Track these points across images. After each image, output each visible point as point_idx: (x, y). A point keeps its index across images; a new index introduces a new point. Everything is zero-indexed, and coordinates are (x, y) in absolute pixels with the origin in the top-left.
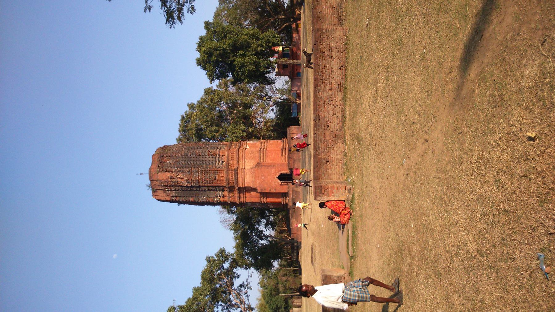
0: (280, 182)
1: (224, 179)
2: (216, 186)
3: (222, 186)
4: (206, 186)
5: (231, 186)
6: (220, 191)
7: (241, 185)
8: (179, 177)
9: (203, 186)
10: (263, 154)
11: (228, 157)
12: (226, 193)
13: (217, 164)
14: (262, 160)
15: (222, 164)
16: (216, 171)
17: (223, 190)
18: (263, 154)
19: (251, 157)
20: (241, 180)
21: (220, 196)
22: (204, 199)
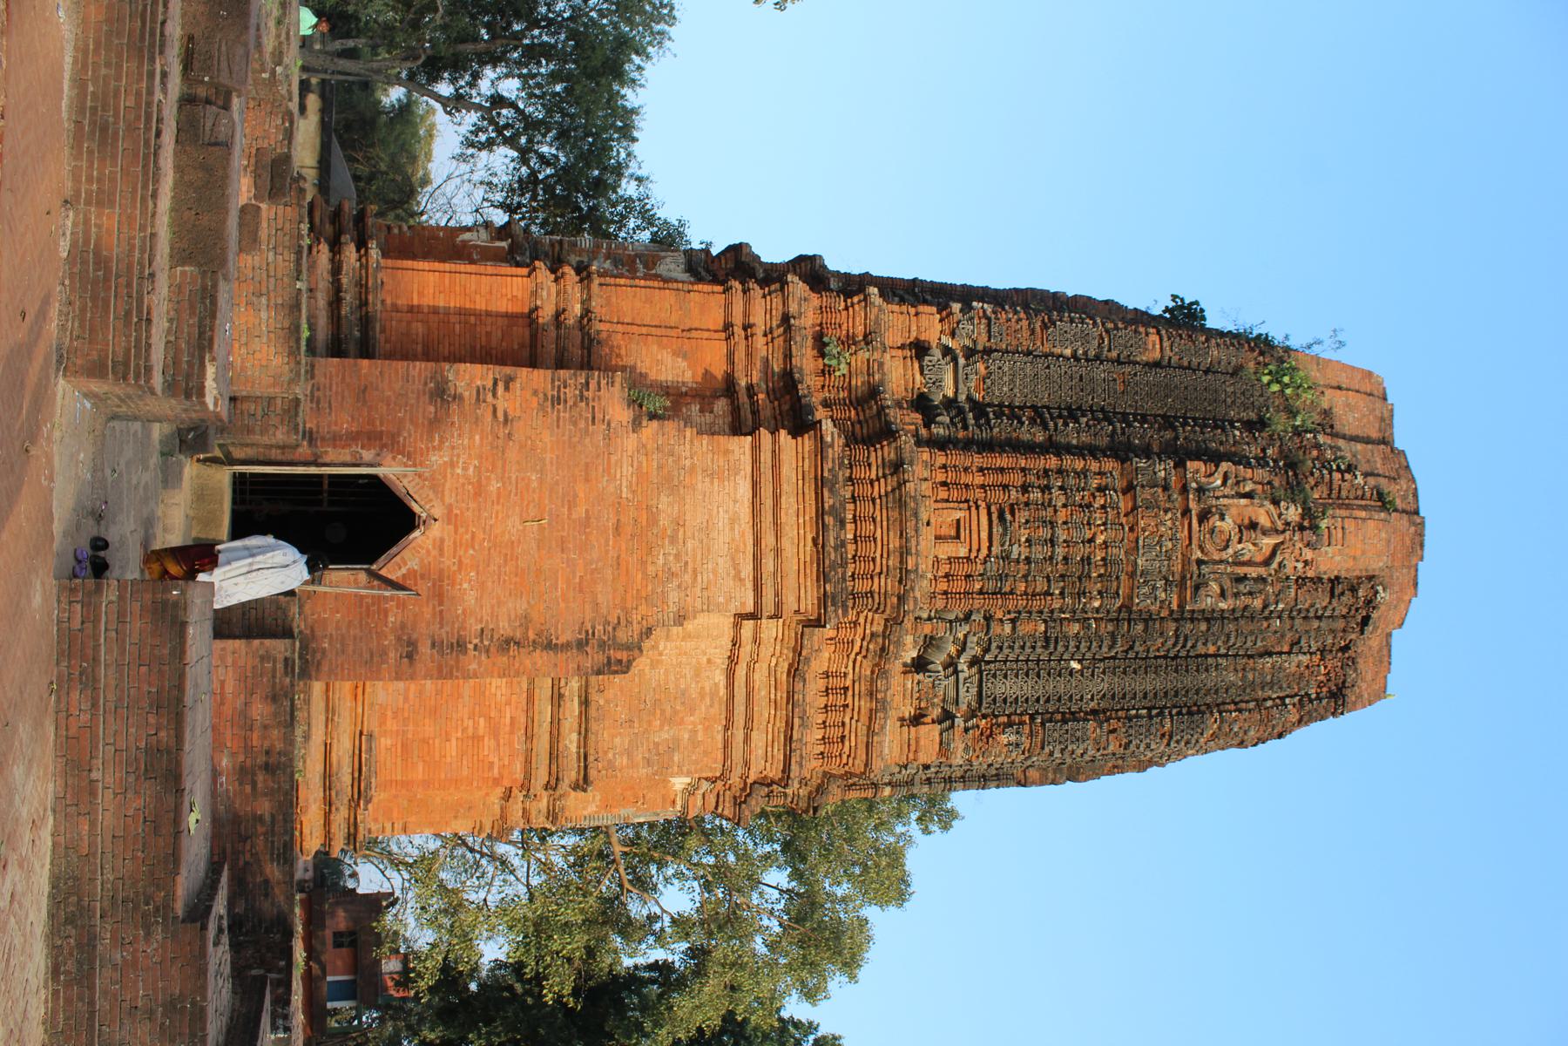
0: (390, 470)
1: (936, 516)
2: (987, 446)
3: (941, 444)
5: (870, 441)
6: (950, 403)
7: (791, 450)
8: (1268, 542)
9: (1092, 451)
10: (554, 755)
11: (880, 706)
12: (899, 377)
13: (974, 649)
14: (573, 686)
15: (930, 642)
17: (921, 403)
18: (554, 755)
19: (669, 721)
20: (789, 502)
21: (947, 351)
22: (1065, 341)
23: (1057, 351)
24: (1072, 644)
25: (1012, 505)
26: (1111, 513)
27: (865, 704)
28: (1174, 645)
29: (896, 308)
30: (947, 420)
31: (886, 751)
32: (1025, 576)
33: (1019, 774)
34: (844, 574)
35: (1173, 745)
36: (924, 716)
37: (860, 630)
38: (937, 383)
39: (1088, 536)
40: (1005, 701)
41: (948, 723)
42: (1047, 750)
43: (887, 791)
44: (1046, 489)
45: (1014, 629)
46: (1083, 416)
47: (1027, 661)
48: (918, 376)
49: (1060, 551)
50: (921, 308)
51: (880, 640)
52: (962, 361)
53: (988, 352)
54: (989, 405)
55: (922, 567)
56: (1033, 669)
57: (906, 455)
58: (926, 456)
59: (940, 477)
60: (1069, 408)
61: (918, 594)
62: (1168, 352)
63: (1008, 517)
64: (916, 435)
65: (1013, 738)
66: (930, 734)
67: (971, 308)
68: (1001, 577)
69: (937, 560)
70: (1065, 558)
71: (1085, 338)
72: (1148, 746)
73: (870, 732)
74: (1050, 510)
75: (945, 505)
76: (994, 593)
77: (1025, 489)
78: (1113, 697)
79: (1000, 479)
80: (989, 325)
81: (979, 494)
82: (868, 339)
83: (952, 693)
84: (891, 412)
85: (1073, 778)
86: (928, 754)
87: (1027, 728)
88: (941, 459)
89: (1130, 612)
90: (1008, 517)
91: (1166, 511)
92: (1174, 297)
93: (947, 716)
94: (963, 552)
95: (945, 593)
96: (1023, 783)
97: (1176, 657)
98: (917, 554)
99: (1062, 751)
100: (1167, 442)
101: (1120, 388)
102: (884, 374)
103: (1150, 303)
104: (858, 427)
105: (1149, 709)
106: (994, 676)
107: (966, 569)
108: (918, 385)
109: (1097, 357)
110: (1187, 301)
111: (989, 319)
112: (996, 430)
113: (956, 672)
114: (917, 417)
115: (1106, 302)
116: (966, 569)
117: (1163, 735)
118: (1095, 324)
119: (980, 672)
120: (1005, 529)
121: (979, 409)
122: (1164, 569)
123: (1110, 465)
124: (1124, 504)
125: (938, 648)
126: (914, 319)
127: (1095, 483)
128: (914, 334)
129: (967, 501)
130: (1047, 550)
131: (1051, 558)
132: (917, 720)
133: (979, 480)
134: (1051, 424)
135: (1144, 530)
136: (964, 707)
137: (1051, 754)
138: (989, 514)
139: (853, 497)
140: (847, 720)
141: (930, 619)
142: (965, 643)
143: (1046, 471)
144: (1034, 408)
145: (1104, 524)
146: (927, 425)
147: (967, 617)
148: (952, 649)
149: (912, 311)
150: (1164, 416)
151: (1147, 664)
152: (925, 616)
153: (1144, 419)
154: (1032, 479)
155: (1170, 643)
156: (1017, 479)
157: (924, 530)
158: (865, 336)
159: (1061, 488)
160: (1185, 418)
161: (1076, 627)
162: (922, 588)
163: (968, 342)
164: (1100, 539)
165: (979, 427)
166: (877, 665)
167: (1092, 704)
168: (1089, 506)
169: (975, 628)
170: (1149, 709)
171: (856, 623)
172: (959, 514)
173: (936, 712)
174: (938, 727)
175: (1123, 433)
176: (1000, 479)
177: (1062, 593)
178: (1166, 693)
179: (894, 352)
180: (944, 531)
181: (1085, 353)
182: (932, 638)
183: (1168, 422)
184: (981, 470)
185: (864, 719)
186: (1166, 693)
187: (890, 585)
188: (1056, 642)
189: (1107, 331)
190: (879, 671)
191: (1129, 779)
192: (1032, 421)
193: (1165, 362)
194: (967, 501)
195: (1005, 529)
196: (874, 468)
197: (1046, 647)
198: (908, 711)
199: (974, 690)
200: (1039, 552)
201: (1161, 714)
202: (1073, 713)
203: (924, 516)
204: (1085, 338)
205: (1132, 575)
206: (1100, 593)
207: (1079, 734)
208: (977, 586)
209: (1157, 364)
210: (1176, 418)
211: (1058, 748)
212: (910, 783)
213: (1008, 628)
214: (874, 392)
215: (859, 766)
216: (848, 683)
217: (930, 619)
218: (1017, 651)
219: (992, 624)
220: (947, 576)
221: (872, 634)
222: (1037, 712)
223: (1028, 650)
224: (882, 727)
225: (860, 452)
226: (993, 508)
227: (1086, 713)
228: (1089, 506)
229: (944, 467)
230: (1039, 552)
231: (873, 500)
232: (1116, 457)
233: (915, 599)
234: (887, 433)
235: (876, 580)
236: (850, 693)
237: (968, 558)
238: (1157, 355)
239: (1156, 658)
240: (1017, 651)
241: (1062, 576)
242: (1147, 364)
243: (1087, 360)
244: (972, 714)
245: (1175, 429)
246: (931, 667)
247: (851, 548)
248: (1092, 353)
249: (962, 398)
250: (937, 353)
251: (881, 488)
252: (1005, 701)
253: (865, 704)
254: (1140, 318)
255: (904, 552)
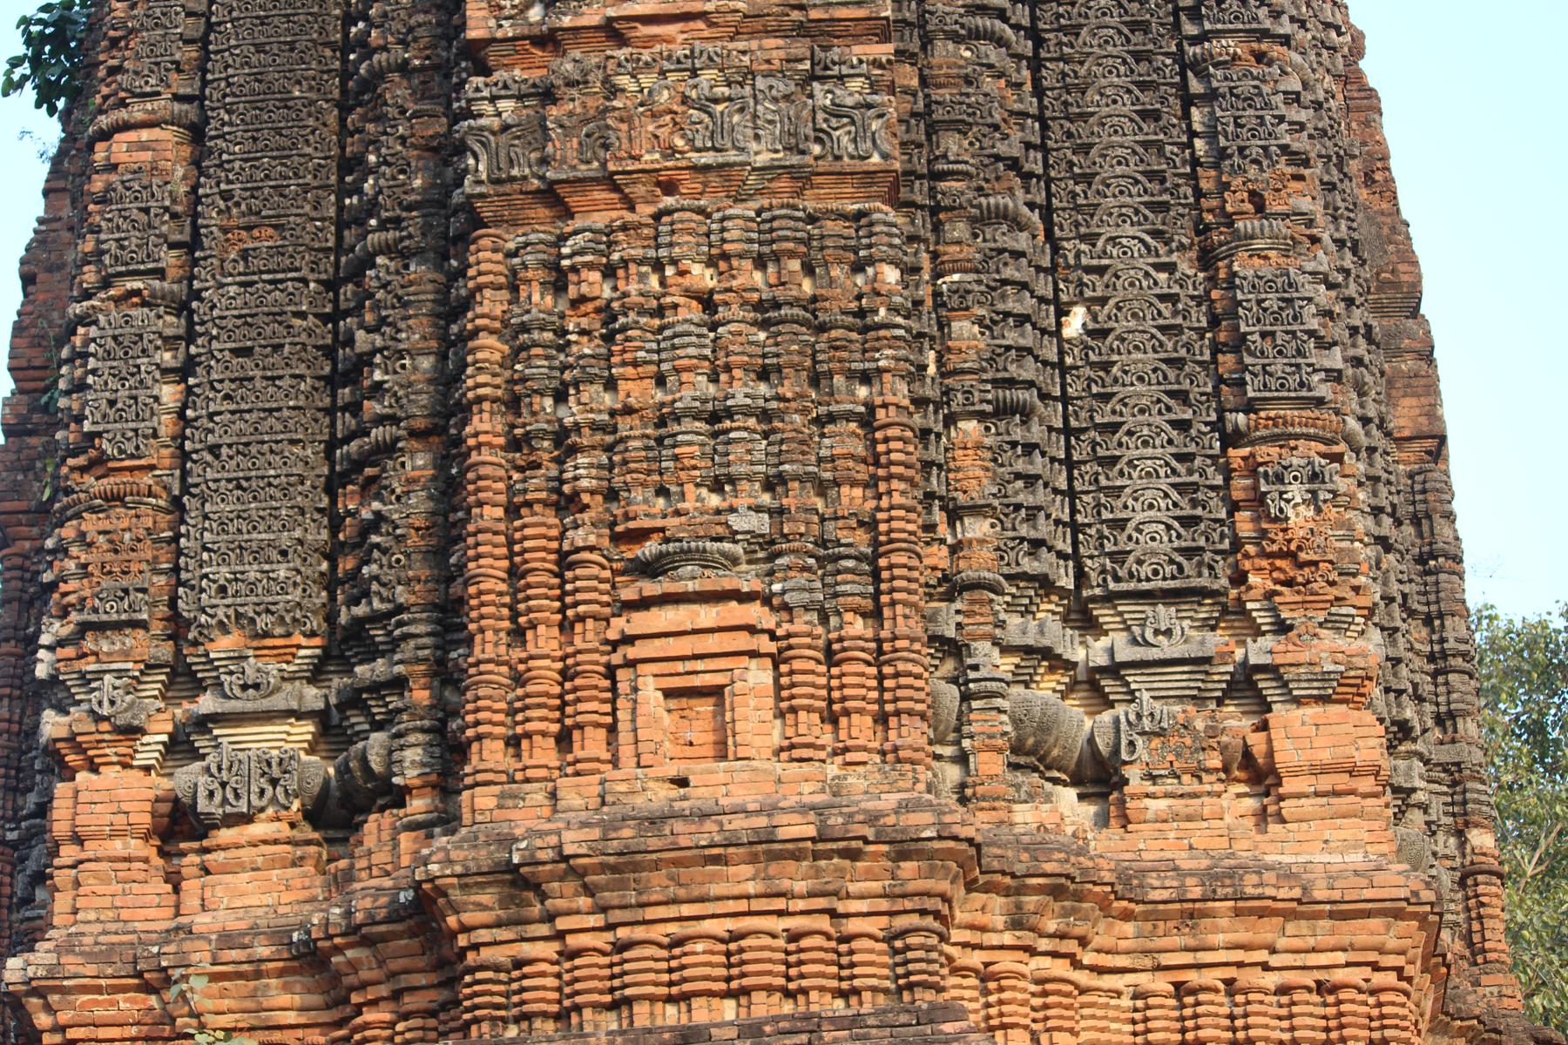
2: (450, 619)
3: (450, 754)
4: (448, 379)
5: (450, 966)
6: (332, 730)
9: (452, 309)
11: (1227, 889)
12: (260, 884)
13: (1045, 625)
15: (1032, 754)
16: (847, 591)
17: (336, 814)
21: (180, 747)
23: (166, 425)
24: (1012, 337)
25: (616, 538)
26: (628, 248)
27: (1223, 931)
28: (1000, 42)
29: (62, 902)
30: (378, 738)
31: (1355, 858)
32: (822, 488)
33: (1404, 461)
34: (838, 1022)
35: (1286, 27)
36: (1247, 754)
37: (1006, 962)
38: (274, 772)
39: (694, 312)
40: (1189, 522)
41: (1265, 684)
42: (1324, 390)
43: (1482, 839)
44: (564, 442)
45: (977, 510)
46: (350, 341)
47: (1069, 463)
48: (258, 829)
49: (744, 391)
50: (60, 828)
51: (1031, 901)
52: (207, 703)
53: (177, 628)
54: (331, 617)
55: (810, 793)
56: (1089, 446)
57: (484, 857)
58: (485, 799)
59: (543, 753)
60: (332, 382)
61: (891, 800)
62: (162, 106)
63: (651, 548)
64: (423, 828)
65: (1296, 491)
66: (1299, 736)
67: (54, 680)
68: (827, 555)
69: (786, 749)
70: (763, 375)
71: (127, 345)
72: (1294, 98)
73: (1302, 909)
74: (624, 424)
75: (624, 736)
76: (876, 575)
77: (567, 503)
78: (1162, 207)
79: (541, 578)
80: (101, 627)
81: (587, 636)
82: (154, 981)
83: (1177, 678)
84: (363, 905)
85: (1401, 296)
86: (1355, 734)
87: (1266, 452)
88: (491, 755)
89: (910, 174)
90: (651, 548)
91: (614, 91)
92: (12, 86)
93: (1246, 686)
94: (759, 675)
95: (882, 719)
96: (1436, 446)
97: (1039, 42)
98: (769, 810)
99: (1325, 345)
100: (422, 94)
101: (266, 239)
102: (254, 930)
103: (31, 149)
104: (410, 1002)
105: (1188, 101)
106: (1119, 557)
107: (807, 663)
108: (282, 830)
109: (182, 308)
110: (20, 49)
111: (84, 628)
112: (402, 595)
113: (1115, 669)
114: (375, 827)
115: (28, 280)
116: (807, 663)
117: (1260, 57)
118: (86, 320)
119: (1110, 598)
120: (687, 555)
121: (344, 645)
122: (781, 87)
123: (486, 260)
124: (598, 213)
125: (1044, 728)
126: (92, 848)
127: (539, 300)
128: (136, 847)
129: (611, 672)
130: (743, 429)
131: (765, 416)
132: (1260, 775)
133: (546, 640)
134: (377, 433)
135: (670, 152)
136: (1216, 641)
137: (1335, 376)
138: (644, 604)
139: (614, 1006)
140: (1271, 980)
141: (962, 759)
142: (1028, 650)
143: (514, 444)
144: (332, 487)
145: (658, 266)
146: (398, 797)
147: (952, 648)
148: (1047, 687)
149: (68, 853)
150: (344, 109)
151: (1055, 116)
152: (953, 773)
153: (351, 165)
154: (536, 485)
155: (993, 54)
156: (540, 524)
157: (699, 795)
158: (148, 988)
159: (560, 397)
160: (346, 46)
161: (963, 329)
162: (869, 790)
163: (154, 685)
164: (703, 276)
165: (395, 644)
166: (1105, 908)
167: (1185, 267)
168: (608, 314)
169: (979, 624)
170: (1188, 101)
171: (986, 976)
172: (650, 692)
173: (1236, 721)
174: (1281, 713)
175: (397, 222)
176: (541, 578)
177: (865, 378)
178: (1139, 56)
179: (191, 901)
180: (700, 729)
181: (169, 342)
182: (1016, 749)
183: (358, 94)
184: (518, 635)
185: (1266, 930)
186: (1139, 56)
187: (864, 885)
188: (1011, 383)
189: (106, 284)
190: (1125, 894)
191: (1403, 133)
192: (372, 488)
193: (190, 111)
194: (611, 672)
195: (687, 555)
196: (527, 950)
197: (1026, 413)
198: (1237, 803)
199: (1164, 614)
200: (748, 452)
201: (1198, 67)
202: (1214, 322)
203: (660, 796)
204: (127, 345)
205: (803, 178)
206: (858, 268)
207: (1272, 302)
208: (858, 626)
209: (196, 133)
210: (346, 74)
211: (1316, 357)
212: (1454, 775)
213: (977, 528)
214: (309, 959)
215: (1401, 936)
216: (1162, 983)
217: (962, 759)
218: (1041, 496)
219: (969, 574)
220: (832, 719)
221: (1016, 924)
222: (1218, 426)
223: (1038, 465)
224: (1287, 875)
225: (483, 991)
226: (628, 594)
227: (1212, 280)
228: (608, 314)
229: (514, 742)
230: (748, 452)
231: (621, 947)
232: (463, 240)
233: (904, 807)
234: (422, 912)
235: (853, 926)
236: (1192, 977)
237: (777, 660)
238: (166, 135)
239: (1039, 91)
240: (1041, 496)
241: (815, 381)
242: (196, 163)
243: (190, 337)
244: (1234, 614)
245: (378, 75)
246: (1103, 744)
247: (764, 1006)
248: (172, 324)
249: (313, 696)
250: (188, 777)
251: (584, 925)
252: (1189, 522)
253: (1223, 931)
254: (69, 175)
255: (766, 848)
